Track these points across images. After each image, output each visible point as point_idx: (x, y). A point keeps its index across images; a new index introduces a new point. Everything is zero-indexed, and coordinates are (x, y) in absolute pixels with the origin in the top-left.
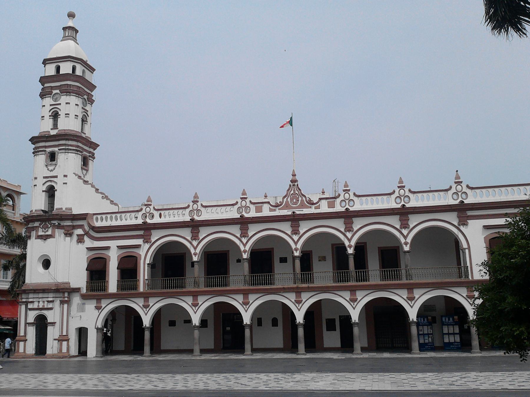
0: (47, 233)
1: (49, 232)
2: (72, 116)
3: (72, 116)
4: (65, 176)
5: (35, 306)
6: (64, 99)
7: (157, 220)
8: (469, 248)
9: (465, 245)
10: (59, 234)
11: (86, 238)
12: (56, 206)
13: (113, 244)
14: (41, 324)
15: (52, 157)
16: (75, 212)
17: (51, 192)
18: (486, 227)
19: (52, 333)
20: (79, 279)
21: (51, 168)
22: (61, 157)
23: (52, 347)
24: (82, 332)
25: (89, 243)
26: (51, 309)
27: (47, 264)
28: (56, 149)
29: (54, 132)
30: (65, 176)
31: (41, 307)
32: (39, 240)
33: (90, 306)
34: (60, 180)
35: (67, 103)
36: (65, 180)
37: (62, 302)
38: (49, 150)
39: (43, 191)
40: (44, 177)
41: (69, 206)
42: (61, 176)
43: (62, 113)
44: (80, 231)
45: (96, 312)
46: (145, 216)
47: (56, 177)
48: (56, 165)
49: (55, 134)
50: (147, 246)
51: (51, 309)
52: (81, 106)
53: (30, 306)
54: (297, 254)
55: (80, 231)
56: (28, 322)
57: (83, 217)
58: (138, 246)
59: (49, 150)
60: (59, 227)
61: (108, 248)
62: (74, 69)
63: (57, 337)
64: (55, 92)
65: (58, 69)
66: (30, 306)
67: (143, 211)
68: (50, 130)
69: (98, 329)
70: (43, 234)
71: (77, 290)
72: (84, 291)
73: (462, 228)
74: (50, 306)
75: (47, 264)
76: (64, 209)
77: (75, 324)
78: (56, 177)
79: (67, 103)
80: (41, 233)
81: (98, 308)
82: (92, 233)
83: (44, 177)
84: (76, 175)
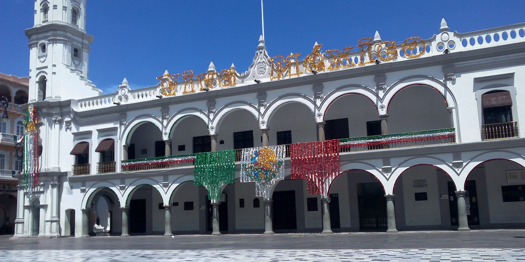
2: (60, 7)
4: (54, 66)
8: (456, 108)
9: (451, 104)
15: (44, 48)
17: (43, 83)
18: (477, 81)
20: (67, 164)
24: (71, 213)
30: (54, 66)
36: (54, 70)
38: (41, 42)
41: (57, 94)
42: (50, 66)
45: (82, 195)
47: (46, 67)
48: (46, 56)
54: (320, 120)
56: (26, 205)
57: (68, 103)
58: (115, 129)
59: (41, 42)
61: (90, 133)
63: (48, 219)
69: (83, 211)
72: (71, 175)
73: (449, 84)
74: (42, 190)
76: (54, 97)
77: (65, 207)
78: (46, 67)
81: (83, 191)
82: (78, 119)
83: (38, 69)
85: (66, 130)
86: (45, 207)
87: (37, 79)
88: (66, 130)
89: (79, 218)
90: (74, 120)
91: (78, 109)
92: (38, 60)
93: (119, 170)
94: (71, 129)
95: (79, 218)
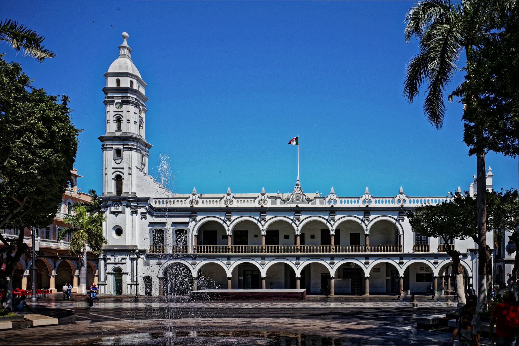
0: (118, 210)
1: (120, 209)
3: (132, 122)
4: (130, 168)
5: (112, 261)
6: (125, 107)
7: (200, 205)
10: (128, 210)
11: (148, 215)
12: (124, 190)
13: (169, 221)
14: (118, 273)
15: (118, 152)
16: (139, 195)
19: (127, 279)
21: (118, 161)
22: (126, 154)
23: (127, 290)
25: (150, 219)
26: (125, 263)
27: (119, 231)
28: (121, 147)
29: (118, 134)
30: (130, 168)
31: (117, 262)
32: (112, 215)
33: (153, 262)
34: (126, 171)
35: (128, 111)
37: (132, 260)
38: (114, 147)
39: (113, 179)
40: (113, 168)
41: (134, 191)
43: (124, 119)
44: (143, 210)
46: (192, 202)
47: (123, 169)
49: (119, 135)
50: (194, 223)
51: (125, 263)
52: (138, 114)
53: (108, 261)
55: (143, 210)
60: (127, 206)
61: (164, 224)
62: (132, 82)
64: (117, 101)
65: (118, 82)
66: (108, 261)
67: (191, 199)
68: (114, 131)
70: (115, 210)
71: (143, 251)
74: (124, 261)
75: (119, 231)
76: (130, 193)
78: (123, 169)
79: (128, 111)
80: (113, 209)
81: (159, 264)
82: (152, 211)
83: (113, 168)
84: (138, 168)
85: (142, 219)
86: (126, 274)
87: (113, 176)
88: (142, 219)
89: (156, 284)
90: (149, 213)
91: (153, 205)
92: (113, 162)
93: (191, 251)
94: (146, 219)
95: (156, 284)
